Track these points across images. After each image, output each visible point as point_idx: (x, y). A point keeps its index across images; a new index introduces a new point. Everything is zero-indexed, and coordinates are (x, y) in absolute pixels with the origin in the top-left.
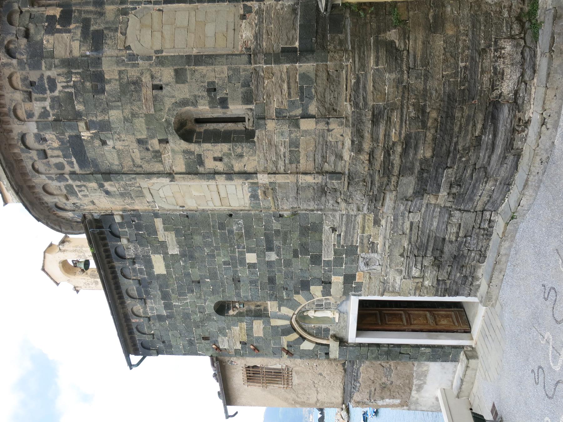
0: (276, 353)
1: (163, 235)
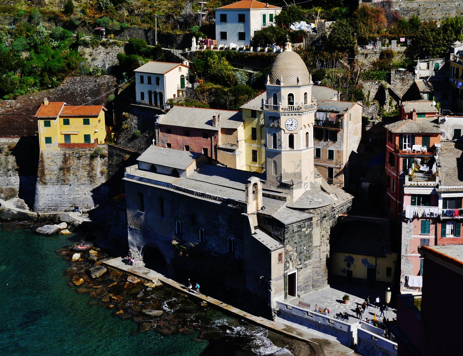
0: (286, 259)
1: (309, 230)
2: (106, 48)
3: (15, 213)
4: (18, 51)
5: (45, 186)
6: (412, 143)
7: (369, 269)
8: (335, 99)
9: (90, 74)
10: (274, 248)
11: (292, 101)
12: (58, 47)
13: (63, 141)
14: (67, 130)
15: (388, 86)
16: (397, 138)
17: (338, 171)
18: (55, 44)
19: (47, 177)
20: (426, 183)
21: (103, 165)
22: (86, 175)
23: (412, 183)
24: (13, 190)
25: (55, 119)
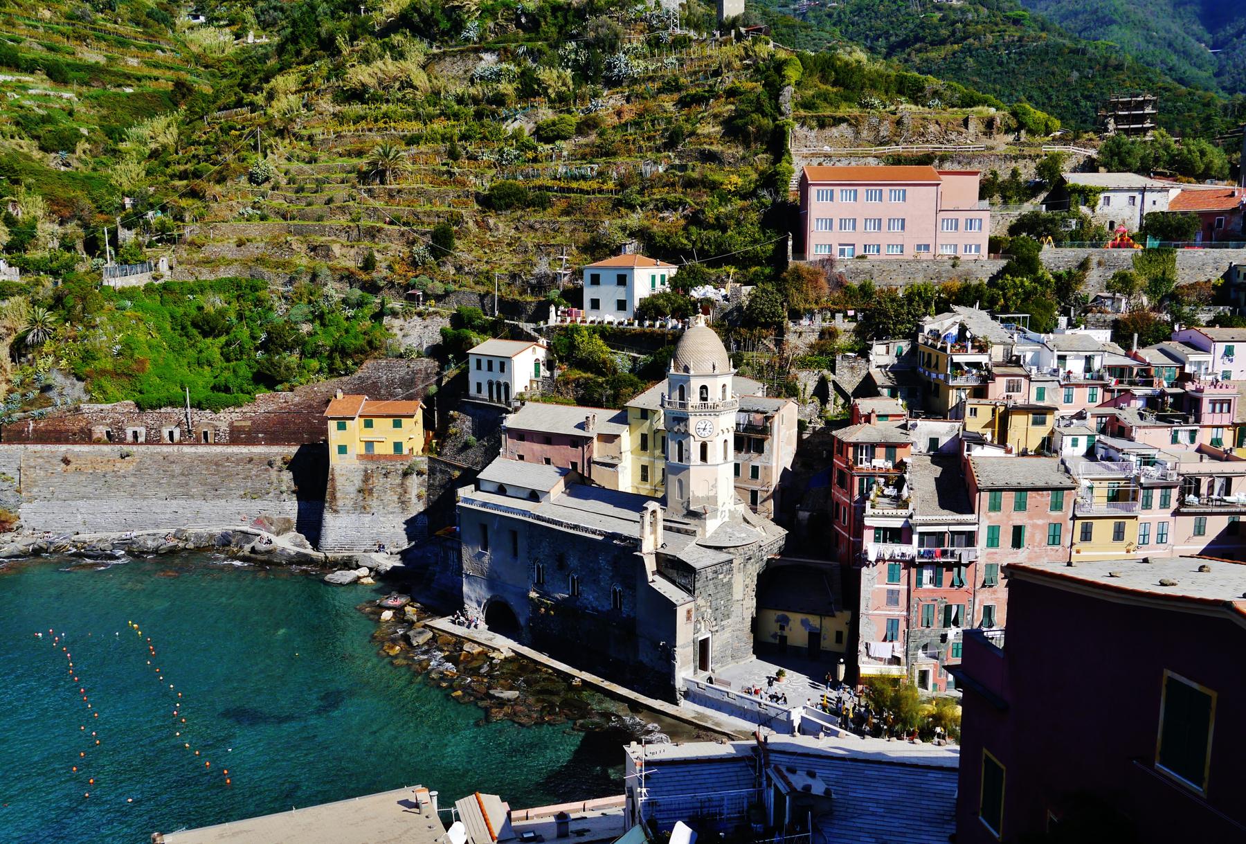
1: (728, 577)
2: (424, 319)
3: (293, 553)
4: (296, 323)
6: (872, 456)
7: (810, 634)
8: (760, 394)
9: (401, 356)
10: (681, 601)
11: (705, 396)
12: (354, 317)
13: (363, 452)
14: (369, 434)
15: (832, 377)
16: (851, 450)
17: (765, 495)
18: (351, 313)
19: (340, 503)
20: (894, 512)
21: (421, 485)
22: (395, 498)
23: (876, 511)
24: (288, 521)
25: (353, 419)
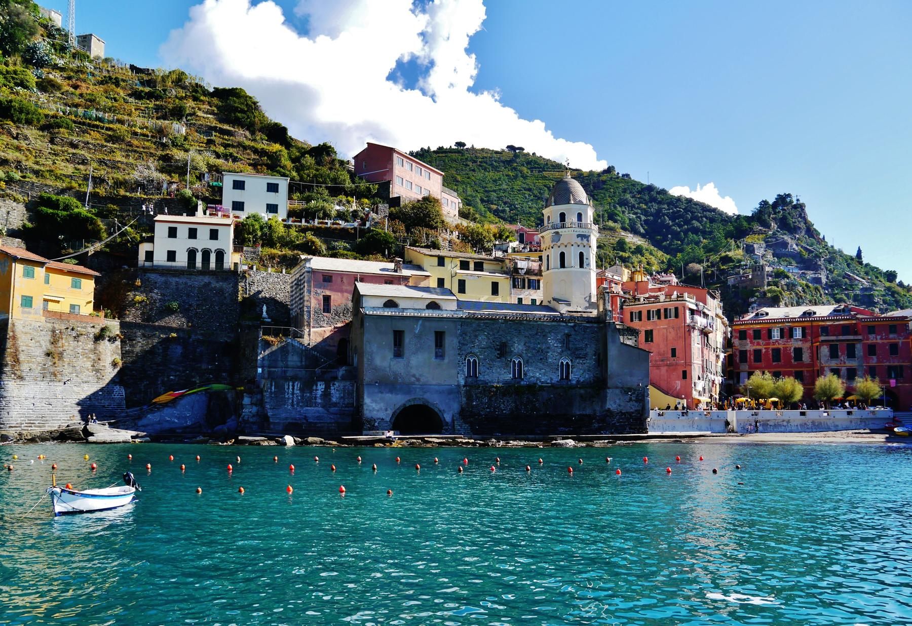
5: (21, 383)
19: (25, 367)
22: (90, 367)
